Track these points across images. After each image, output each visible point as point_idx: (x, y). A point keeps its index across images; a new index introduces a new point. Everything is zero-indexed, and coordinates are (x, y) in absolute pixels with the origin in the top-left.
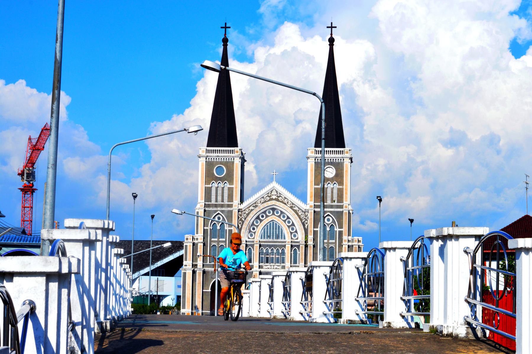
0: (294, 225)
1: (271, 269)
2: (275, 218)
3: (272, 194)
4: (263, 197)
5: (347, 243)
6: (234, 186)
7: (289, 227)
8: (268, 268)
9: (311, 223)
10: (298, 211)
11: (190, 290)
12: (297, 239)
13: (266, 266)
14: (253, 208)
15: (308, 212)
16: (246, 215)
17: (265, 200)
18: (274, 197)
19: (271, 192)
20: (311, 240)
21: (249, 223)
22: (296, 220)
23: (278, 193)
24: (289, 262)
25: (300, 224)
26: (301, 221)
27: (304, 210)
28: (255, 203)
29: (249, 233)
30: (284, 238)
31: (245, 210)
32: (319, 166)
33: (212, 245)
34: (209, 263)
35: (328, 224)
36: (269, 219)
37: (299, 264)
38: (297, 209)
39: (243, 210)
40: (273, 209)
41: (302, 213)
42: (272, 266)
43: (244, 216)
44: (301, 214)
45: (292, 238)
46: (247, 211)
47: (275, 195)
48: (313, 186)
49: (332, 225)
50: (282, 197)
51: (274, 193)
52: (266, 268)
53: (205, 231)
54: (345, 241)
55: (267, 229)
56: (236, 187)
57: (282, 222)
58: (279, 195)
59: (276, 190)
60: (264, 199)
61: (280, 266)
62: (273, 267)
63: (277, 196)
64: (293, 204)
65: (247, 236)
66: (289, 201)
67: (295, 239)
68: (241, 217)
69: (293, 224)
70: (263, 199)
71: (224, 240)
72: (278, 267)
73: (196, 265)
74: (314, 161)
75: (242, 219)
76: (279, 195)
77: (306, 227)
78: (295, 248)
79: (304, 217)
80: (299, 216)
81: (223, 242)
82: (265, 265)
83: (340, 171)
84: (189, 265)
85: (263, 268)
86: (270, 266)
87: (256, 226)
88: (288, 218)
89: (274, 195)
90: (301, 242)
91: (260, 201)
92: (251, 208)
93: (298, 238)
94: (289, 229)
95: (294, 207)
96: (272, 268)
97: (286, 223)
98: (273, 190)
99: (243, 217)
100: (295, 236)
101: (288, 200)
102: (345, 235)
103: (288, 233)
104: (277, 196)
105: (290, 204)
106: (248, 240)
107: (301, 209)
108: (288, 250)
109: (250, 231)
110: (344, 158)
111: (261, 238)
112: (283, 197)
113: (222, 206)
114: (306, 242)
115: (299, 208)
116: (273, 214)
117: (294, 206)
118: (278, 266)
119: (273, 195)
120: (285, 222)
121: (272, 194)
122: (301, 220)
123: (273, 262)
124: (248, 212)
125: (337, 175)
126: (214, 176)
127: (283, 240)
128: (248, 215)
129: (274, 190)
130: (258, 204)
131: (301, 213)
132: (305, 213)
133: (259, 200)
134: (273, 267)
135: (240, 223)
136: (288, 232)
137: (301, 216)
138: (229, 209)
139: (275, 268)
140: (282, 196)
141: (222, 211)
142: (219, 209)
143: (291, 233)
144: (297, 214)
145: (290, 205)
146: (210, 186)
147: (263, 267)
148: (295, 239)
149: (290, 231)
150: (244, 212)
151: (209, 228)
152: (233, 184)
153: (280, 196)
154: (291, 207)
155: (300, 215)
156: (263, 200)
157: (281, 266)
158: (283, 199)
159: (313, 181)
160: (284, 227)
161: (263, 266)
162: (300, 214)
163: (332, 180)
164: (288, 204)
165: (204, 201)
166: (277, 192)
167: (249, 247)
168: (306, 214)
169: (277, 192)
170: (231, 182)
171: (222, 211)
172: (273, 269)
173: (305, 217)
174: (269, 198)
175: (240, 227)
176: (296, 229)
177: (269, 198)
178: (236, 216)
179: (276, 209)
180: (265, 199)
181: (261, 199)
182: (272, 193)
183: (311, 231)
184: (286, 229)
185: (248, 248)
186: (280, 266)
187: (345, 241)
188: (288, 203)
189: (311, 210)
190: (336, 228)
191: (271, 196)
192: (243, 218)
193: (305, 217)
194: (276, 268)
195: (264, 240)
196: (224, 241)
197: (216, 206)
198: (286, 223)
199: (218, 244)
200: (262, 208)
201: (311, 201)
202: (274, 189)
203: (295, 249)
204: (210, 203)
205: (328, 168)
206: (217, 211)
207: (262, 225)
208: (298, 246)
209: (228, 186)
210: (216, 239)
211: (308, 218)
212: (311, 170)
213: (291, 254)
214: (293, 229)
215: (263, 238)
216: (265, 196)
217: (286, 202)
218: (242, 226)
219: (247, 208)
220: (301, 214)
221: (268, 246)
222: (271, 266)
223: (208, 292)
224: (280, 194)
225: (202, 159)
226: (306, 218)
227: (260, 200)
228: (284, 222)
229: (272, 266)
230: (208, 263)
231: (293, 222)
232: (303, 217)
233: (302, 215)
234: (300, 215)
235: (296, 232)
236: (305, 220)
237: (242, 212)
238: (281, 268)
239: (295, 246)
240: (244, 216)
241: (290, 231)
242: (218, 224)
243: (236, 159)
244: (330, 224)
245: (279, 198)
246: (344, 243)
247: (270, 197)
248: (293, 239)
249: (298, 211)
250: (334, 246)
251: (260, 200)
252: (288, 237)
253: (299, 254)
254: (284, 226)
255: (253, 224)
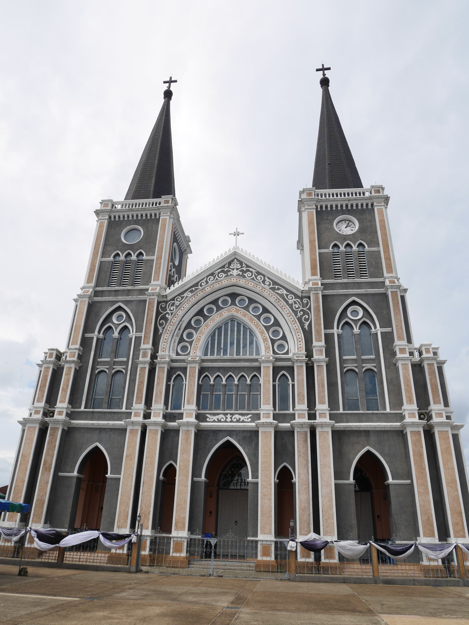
0: (279, 325)
1: (226, 421)
2: (237, 311)
3: (231, 267)
4: (212, 274)
5: (407, 355)
6: (155, 257)
7: (267, 328)
8: (219, 421)
9: (317, 315)
10: (287, 295)
11: (26, 469)
12: (287, 353)
13: (214, 414)
14: (190, 294)
15: (309, 298)
16: (175, 307)
17: (217, 278)
18: (235, 272)
19: (230, 263)
20: (321, 351)
21: (181, 323)
22: (283, 311)
23: (244, 265)
24: (269, 404)
25: (293, 319)
26: (296, 315)
27: (300, 294)
28: (196, 285)
29: (179, 343)
30: (258, 353)
31: (173, 299)
32: (326, 217)
33: (97, 372)
34: (85, 408)
35: (356, 321)
36: (225, 313)
37: (293, 410)
38: (285, 292)
39: (169, 298)
40: (233, 296)
41: (295, 300)
42: (229, 416)
43: (170, 310)
44: (294, 301)
45: (274, 352)
46: (178, 299)
47: (237, 269)
48: (316, 251)
49: (364, 323)
50: (251, 272)
51: (236, 265)
52: (214, 421)
53: (85, 342)
54: (402, 351)
55: (220, 335)
56: (159, 258)
57: (251, 318)
58: (245, 270)
59: (237, 260)
60: (214, 277)
61: (248, 414)
62: (231, 418)
63: (242, 271)
64: (275, 283)
65: (173, 350)
66: (266, 279)
67: (283, 354)
68: (165, 312)
69: (277, 323)
70: (212, 277)
71: (125, 359)
72: (242, 418)
73: (52, 414)
74: (314, 207)
75: (167, 316)
76: (245, 270)
77: (306, 327)
78: (283, 372)
79: (301, 307)
80: (291, 306)
81: (121, 363)
82: (210, 414)
83: (369, 223)
84: (37, 412)
85: (208, 419)
86: (222, 416)
87: (194, 328)
88: (265, 310)
89: (235, 270)
90: (297, 357)
91: (207, 282)
92: (185, 295)
93: (288, 350)
94: (268, 333)
95: (278, 289)
96: (229, 420)
97: (260, 322)
98: (233, 261)
99: (168, 311)
100: (281, 347)
101: (264, 276)
102: (400, 339)
103: (265, 340)
104: (240, 271)
105: (268, 283)
106: (174, 357)
107: (292, 293)
108: (266, 375)
109: (181, 340)
110: (374, 200)
111: (206, 354)
112: (254, 271)
113: (128, 292)
114: (309, 354)
115: (287, 290)
116: (233, 303)
117: (277, 287)
118: (242, 415)
119: (233, 269)
120: (259, 320)
121: (231, 267)
122: (296, 313)
123: (230, 407)
124: (179, 303)
125: (362, 230)
126: (121, 244)
127: (254, 357)
128: (177, 307)
129: (235, 260)
130: (201, 286)
131: (293, 300)
132: (301, 298)
133: (204, 278)
134: (231, 418)
135: (161, 325)
136: (266, 339)
137: (294, 306)
138: (142, 297)
139: (235, 420)
140: (251, 269)
141: (126, 302)
142: (120, 298)
143: (273, 342)
144: (287, 302)
145: (269, 285)
146: (111, 259)
147: (208, 417)
148: (283, 354)
149: (270, 337)
150: (173, 302)
151: (95, 335)
152: (153, 254)
153: (249, 271)
154: (273, 289)
155: (291, 303)
156: (211, 279)
157: (250, 416)
158: (253, 276)
159: (315, 241)
160: (257, 328)
161: (207, 415)
162: (290, 302)
163: (353, 237)
164: (265, 284)
165: (93, 284)
166: (241, 263)
167: (177, 373)
168: (306, 302)
169: (241, 263)
170: (151, 251)
171: (126, 302)
172: (232, 421)
173: (303, 307)
174: (224, 275)
175: (161, 331)
176: (284, 333)
177: (224, 275)
178: (153, 307)
179: (239, 295)
180: (217, 277)
181: (207, 277)
182: (232, 265)
183: (318, 332)
184: (262, 333)
185: (174, 376)
186: (248, 414)
187: (402, 351)
188: (264, 282)
189: (316, 289)
190: (375, 327)
191: (230, 271)
192: (168, 313)
193: (301, 308)
194: (238, 421)
195: (212, 357)
196: (124, 362)
197: (117, 292)
198: (260, 322)
199: (111, 368)
200: (208, 290)
201: (314, 274)
202: (236, 258)
203: (284, 375)
204: (105, 288)
205: (343, 222)
206: (118, 302)
207: (207, 326)
208: (291, 370)
209: (145, 257)
210: (108, 359)
211: (310, 309)
212: (310, 223)
213: (274, 386)
214: (276, 333)
215: (209, 354)
216: (217, 272)
217: (261, 281)
218: (163, 328)
219: (179, 295)
220: (294, 301)
221: (219, 369)
222: (227, 414)
223: (71, 477)
224: (247, 266)
225: (101, 217)
226: (304, 309)
227: (205, 280)
228: (255, 319)
229: (229, 416)
230: (82, 409)
231: (275, 319)
232: (299, 308)
233: (295, 303)
234: (292, 304)
235: (284, 338)
236: (302, 313)
237: (166, 302)
238: (250, 420)
239: (283, 368)
240: (170, 310)
241: (270, 337)
242: (116, 329)
243: (163, 213)
244: (359, 320)
245: (246, 275)
246: (399, 355)
247: (226, 272)
248: (278, 354)
249: (287, 295)
250: (375, 367)
251: (205, 280)
252: (267, 348)
253: (293, 386)
254: (257, 326)
255: (189, 325)
